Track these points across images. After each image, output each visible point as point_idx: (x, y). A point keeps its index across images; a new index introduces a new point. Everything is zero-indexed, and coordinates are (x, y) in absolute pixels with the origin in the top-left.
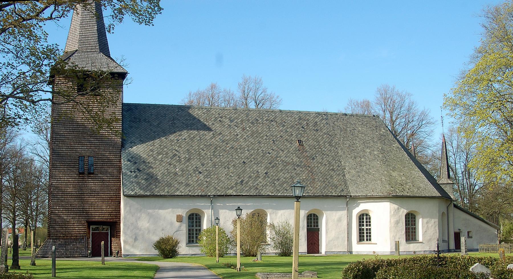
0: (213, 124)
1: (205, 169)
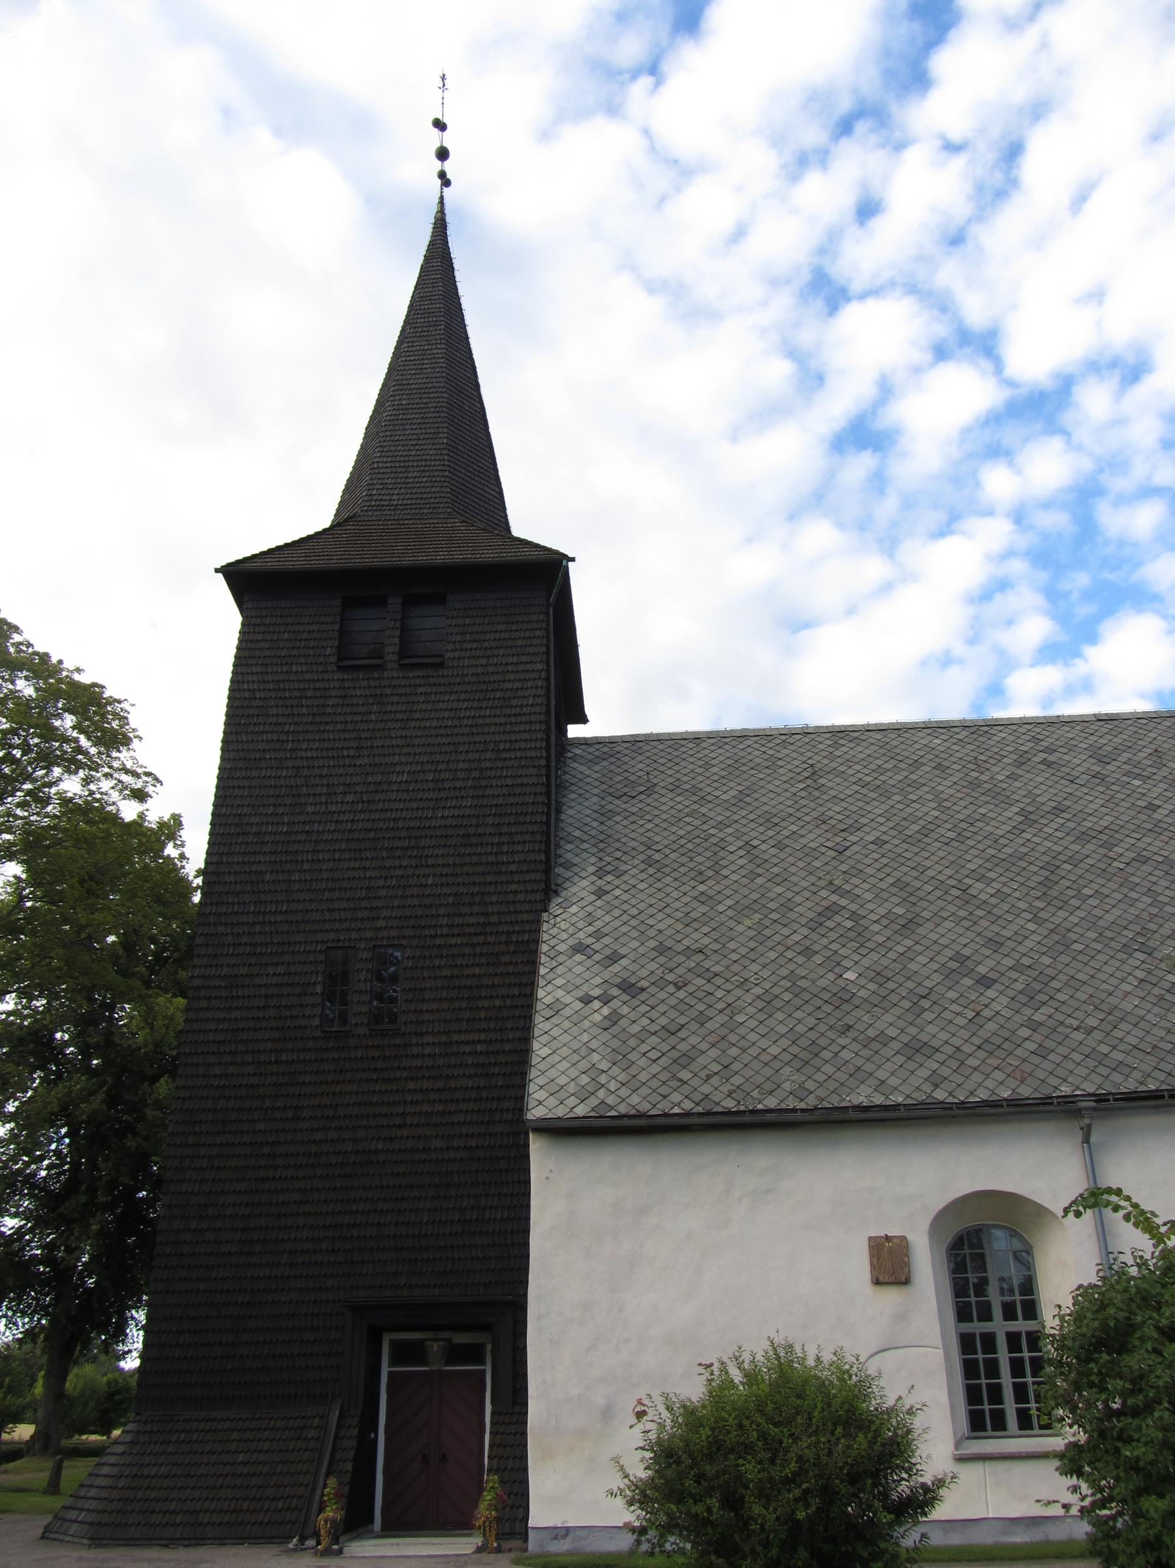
1: (1009, 962)
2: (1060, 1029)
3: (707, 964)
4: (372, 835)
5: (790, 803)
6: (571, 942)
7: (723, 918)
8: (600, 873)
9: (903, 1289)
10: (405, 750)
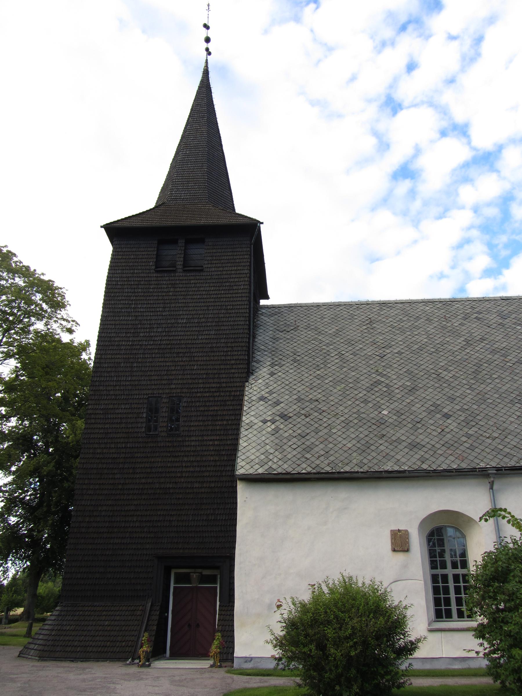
1: (458, 407)
2: (480, 438)
3: (320, 406)
4: (169, 347)
5: (359, 335)
6: (258, 396)
7: (328, 386)
8: (272, 365)
9: (406, 554)
10: (185, 309)
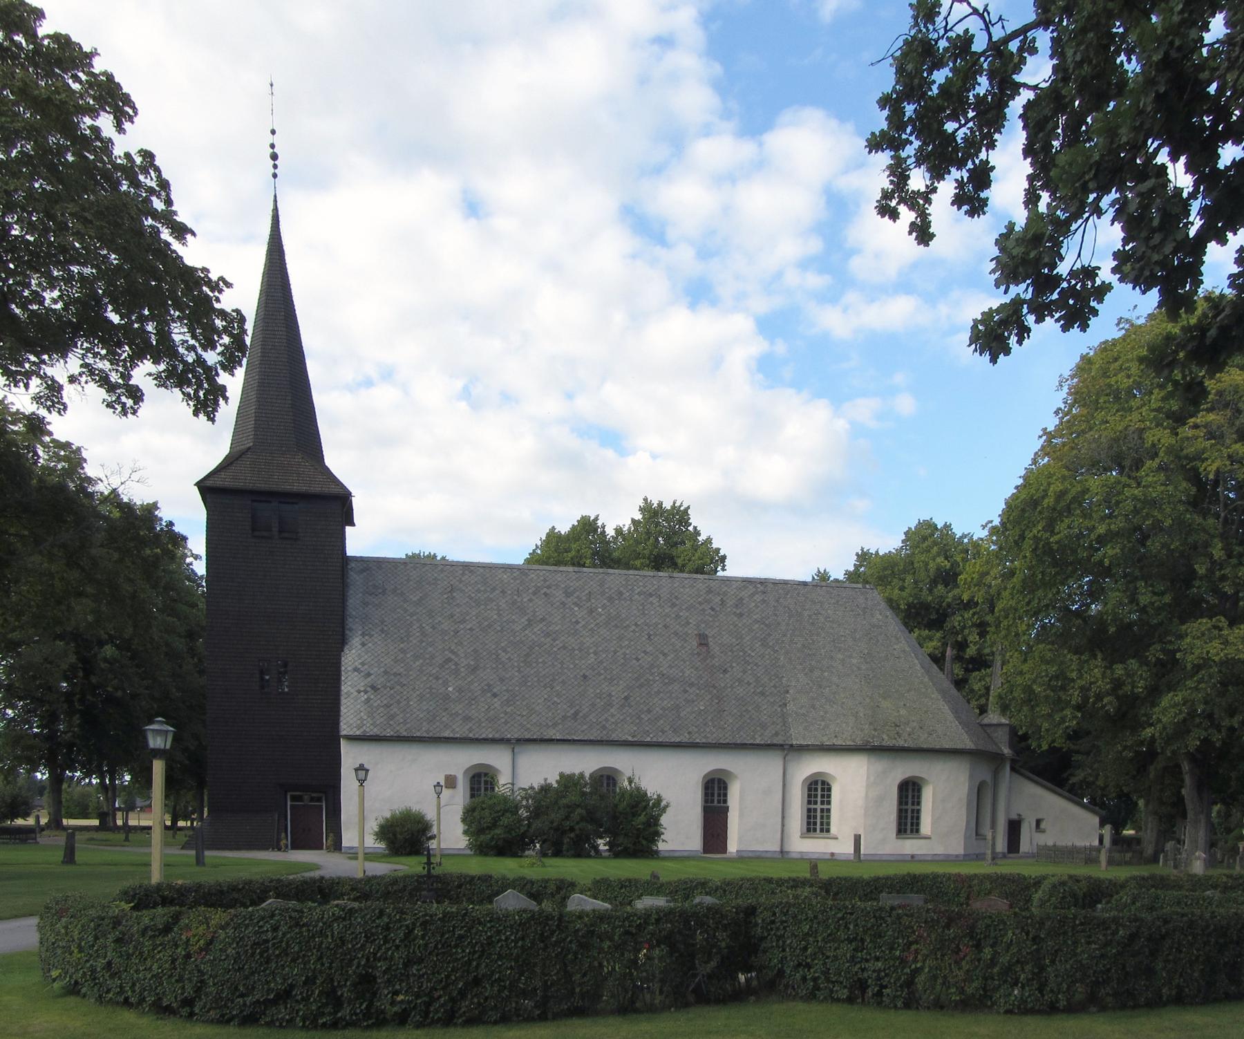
0: (530, 600)
1: (505, 688)
5: (440, 605)
6: (353, 666)
